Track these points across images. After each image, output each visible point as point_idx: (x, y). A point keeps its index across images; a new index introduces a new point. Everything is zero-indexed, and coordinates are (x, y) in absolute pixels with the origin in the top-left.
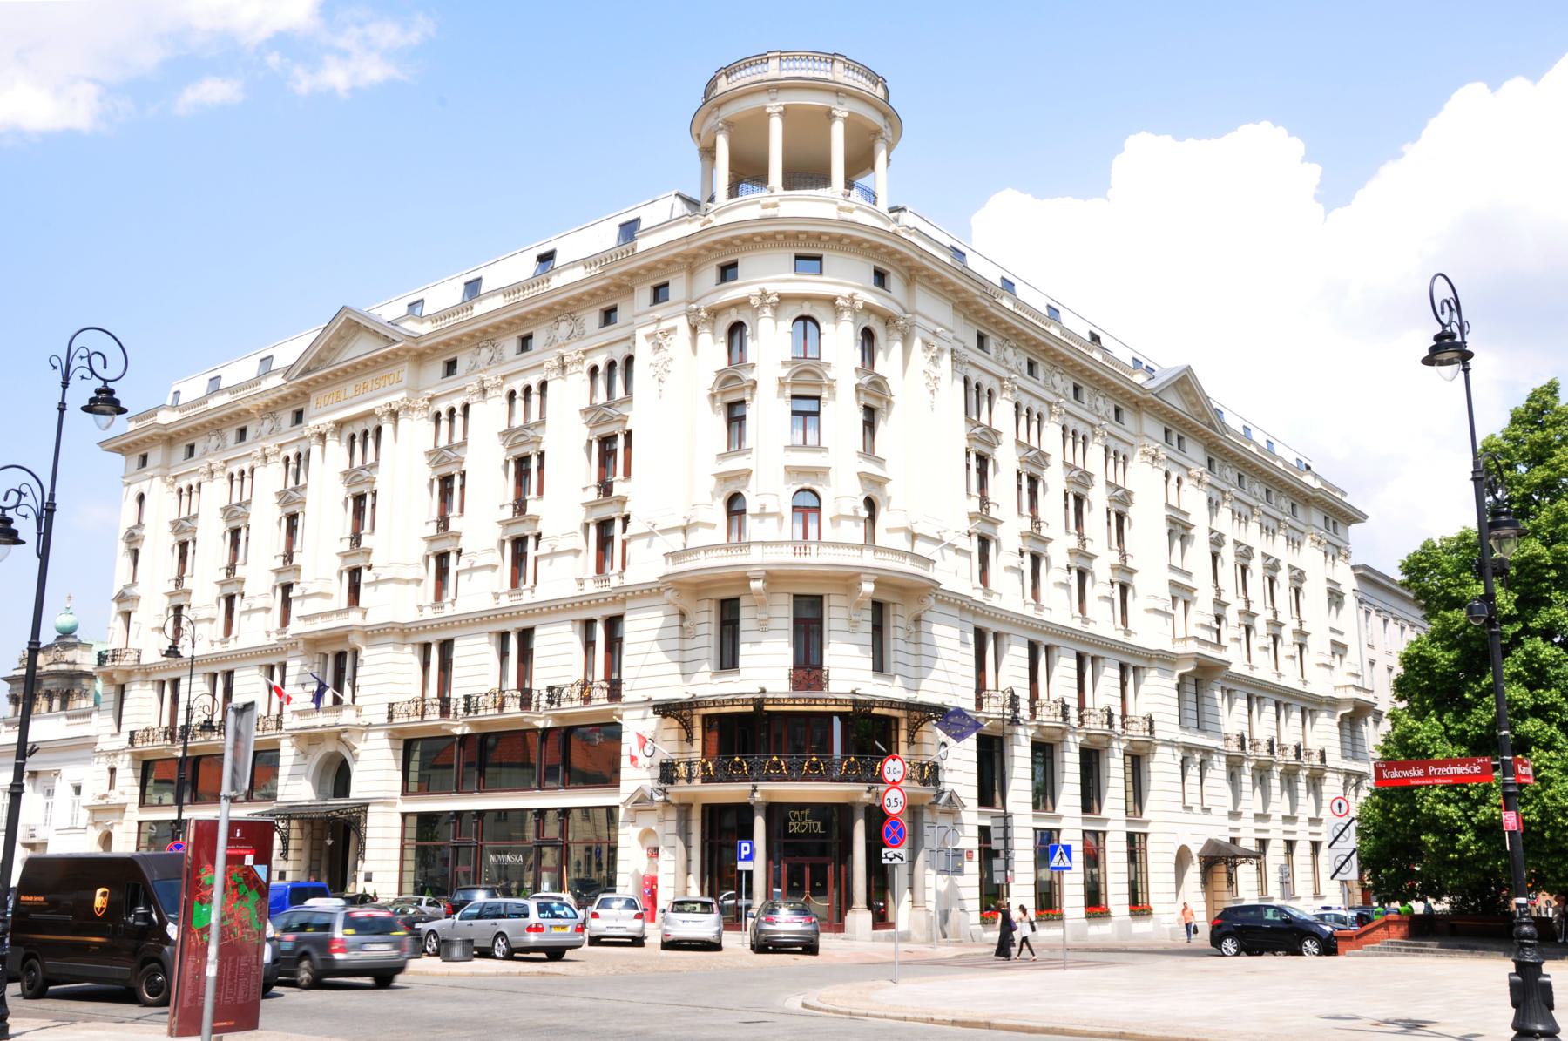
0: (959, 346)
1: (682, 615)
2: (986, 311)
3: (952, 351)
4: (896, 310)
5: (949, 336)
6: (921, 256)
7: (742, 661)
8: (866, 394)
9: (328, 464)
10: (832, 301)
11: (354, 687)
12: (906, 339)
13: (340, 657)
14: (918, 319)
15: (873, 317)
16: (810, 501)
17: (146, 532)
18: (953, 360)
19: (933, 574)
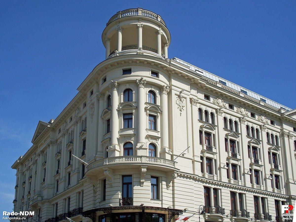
0: (191, 97)
1: (94, 186)
2: (206, 86)
3: (191, 99)
4: (162, 84)
5: (189, 93)
6: (170, 66)
7: (107, 198)
8: (150, 111)
9: (40, 160)
10: (135, 82)
11: (41, 218)
12: (169, 94)
13: (40, 210)
14: (173, 87)
15: (153, 87)
16: (128, 146)
17: (19, 186)
18: (191, 102)
19: (177, 166)
